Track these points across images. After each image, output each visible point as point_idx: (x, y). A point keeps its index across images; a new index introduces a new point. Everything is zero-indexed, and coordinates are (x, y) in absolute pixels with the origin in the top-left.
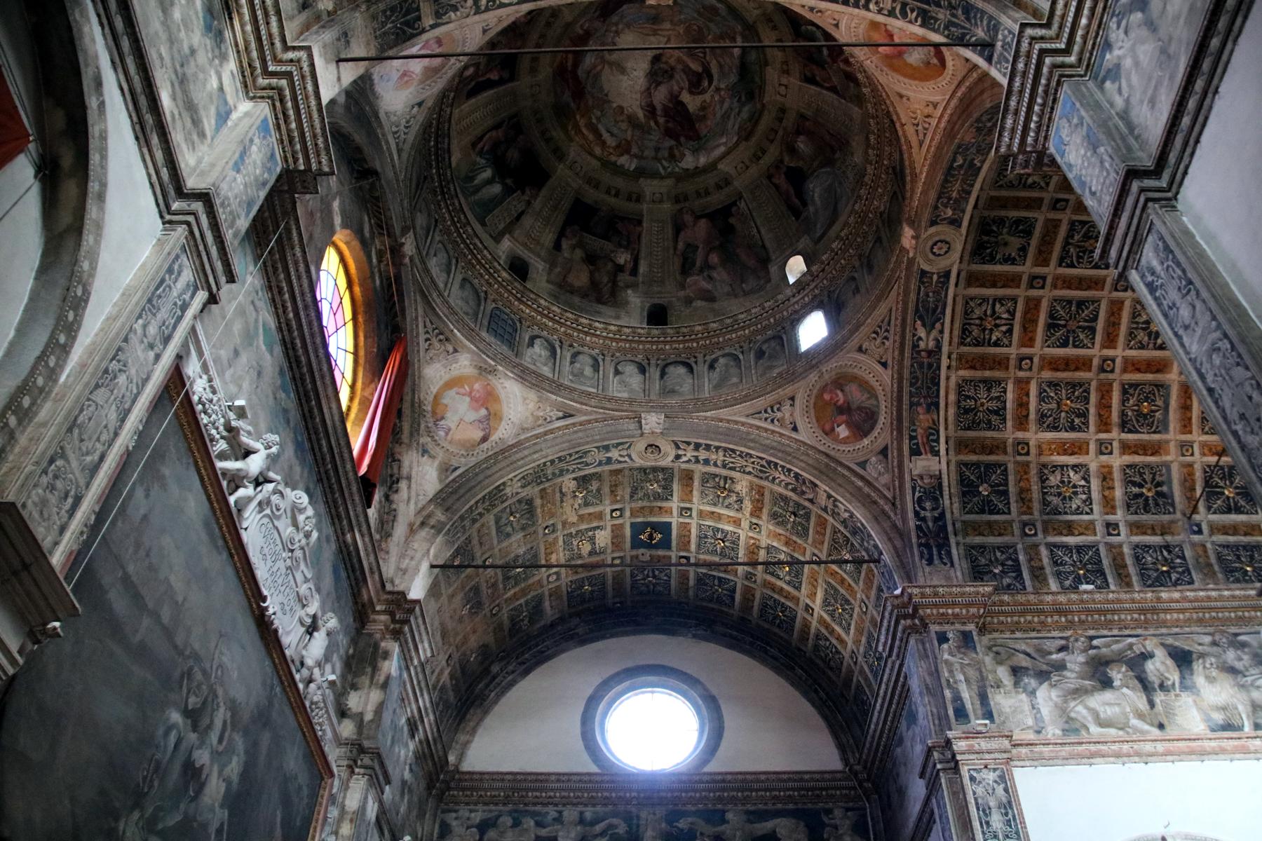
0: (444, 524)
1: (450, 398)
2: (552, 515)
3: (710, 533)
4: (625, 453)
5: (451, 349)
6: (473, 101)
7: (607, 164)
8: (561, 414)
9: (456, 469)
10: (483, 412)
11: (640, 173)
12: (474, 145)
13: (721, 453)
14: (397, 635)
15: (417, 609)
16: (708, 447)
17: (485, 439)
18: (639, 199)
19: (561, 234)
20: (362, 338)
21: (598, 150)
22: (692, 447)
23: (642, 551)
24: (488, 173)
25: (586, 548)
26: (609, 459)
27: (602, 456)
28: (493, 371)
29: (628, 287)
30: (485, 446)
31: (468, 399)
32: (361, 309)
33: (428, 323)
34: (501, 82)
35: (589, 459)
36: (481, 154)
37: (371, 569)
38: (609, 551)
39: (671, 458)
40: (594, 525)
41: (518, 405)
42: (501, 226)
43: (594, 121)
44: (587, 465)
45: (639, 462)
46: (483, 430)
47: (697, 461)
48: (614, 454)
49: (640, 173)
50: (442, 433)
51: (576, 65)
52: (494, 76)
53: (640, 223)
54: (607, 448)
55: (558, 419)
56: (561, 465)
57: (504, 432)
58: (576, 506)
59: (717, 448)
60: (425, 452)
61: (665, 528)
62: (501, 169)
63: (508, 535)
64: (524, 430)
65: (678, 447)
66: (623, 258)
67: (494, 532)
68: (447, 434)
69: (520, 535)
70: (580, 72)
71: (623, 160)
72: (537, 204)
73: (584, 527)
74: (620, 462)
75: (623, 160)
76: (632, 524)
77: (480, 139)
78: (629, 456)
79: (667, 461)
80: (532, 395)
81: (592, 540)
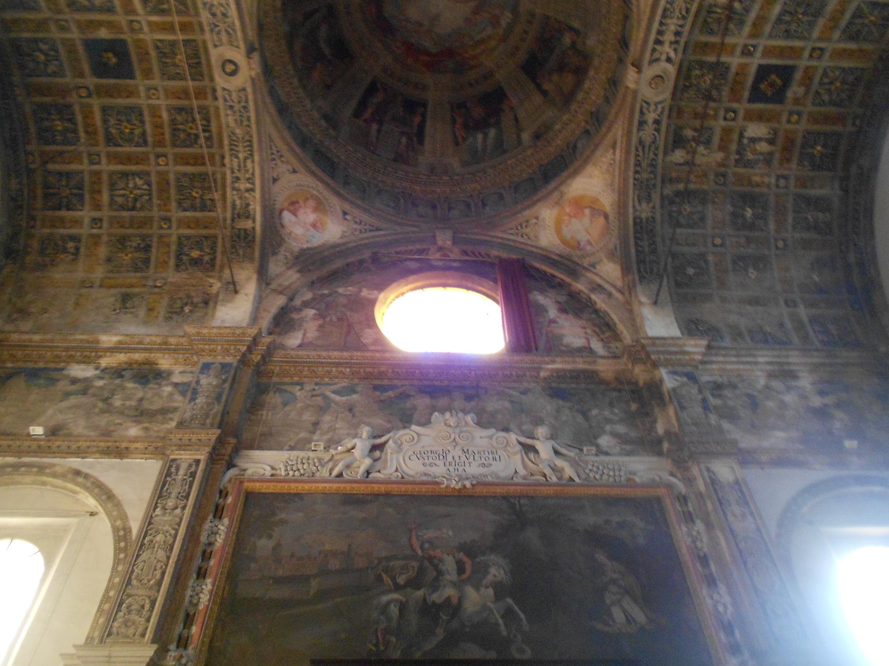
0: (634, 280)
1: (567, 233)
2: (705, 175)
3: (783, 27)
4: (652, 107)
5: (534, 221)
6: (427, 140)
7: (504, 39)
8: (611, 151)
9: (616, 249)
10: (587, 211)
11: (515, 10)
12: (457, 144)
13: (668, 21)
14: (655, 365)
15: (643, 341)
16: (660, 33)
17: (606, 216)
18: (533, 15)
19: (539, 86)
20: (480, 288)
21: (493, 43)
22: (658, 47)
23: (790, 94)
24: (480, 136)
25: (763, 147)
26: (657, 122)
27: (649, 129)
28: (562, 194)
29: (584, 44)
30: (611, 218)
31: (574, 220)
32: (464, 283)
33: (512, 232)
34: (423, 116)
35: (648, 140)
36: (464, 139)
37: (589, 363)
38: (776, 125)
39: (669, 67)
40: (735, 136)
41: (594, 183)
42: (515, 136)
43: (471, 43)
44: (654, 142)
45: (667, 95)
46: (599, 215)
47: (677, 42)
48: (651, 117)
49: (515, 10)
50: (588, 248)
51: (429, 54)
52: (417, 120)
53: (548, 18)
54: (642, 123)
55: (614, 154)
56: (644, 165)
57: (607, 201)
58: (705, 152)
59: (661, 24)
60: (593, 265)
61: (763, 72)
62: (480, 125)
63: (703, 219)
64: (612, 185)
65: (657, 60)
66: (567, 40)
67: (690, 231)
68: (590, 244)
69: (710, 206)
70: (434, 50)
71: (503, 23)
72: (514, 102)
73: (734, 147)
74: (662, 112)
75: (503, 23)
76: (750, 101)
77: (455, 137)
78: (656, 104)
79: (671, 69)
80: (590, 169)
81: (753, 140)
